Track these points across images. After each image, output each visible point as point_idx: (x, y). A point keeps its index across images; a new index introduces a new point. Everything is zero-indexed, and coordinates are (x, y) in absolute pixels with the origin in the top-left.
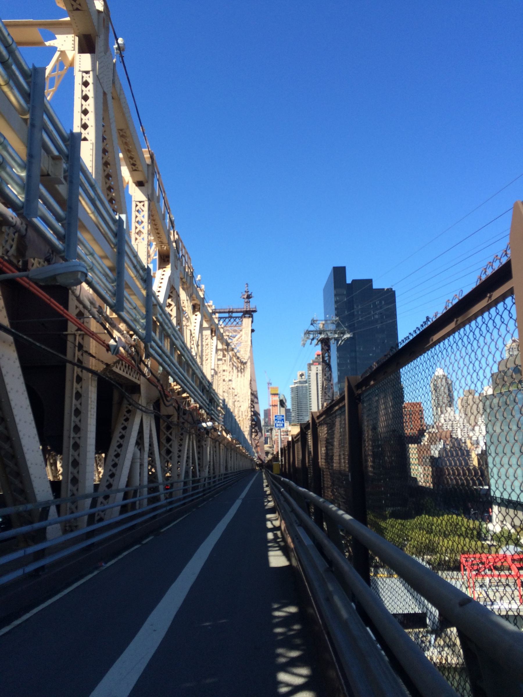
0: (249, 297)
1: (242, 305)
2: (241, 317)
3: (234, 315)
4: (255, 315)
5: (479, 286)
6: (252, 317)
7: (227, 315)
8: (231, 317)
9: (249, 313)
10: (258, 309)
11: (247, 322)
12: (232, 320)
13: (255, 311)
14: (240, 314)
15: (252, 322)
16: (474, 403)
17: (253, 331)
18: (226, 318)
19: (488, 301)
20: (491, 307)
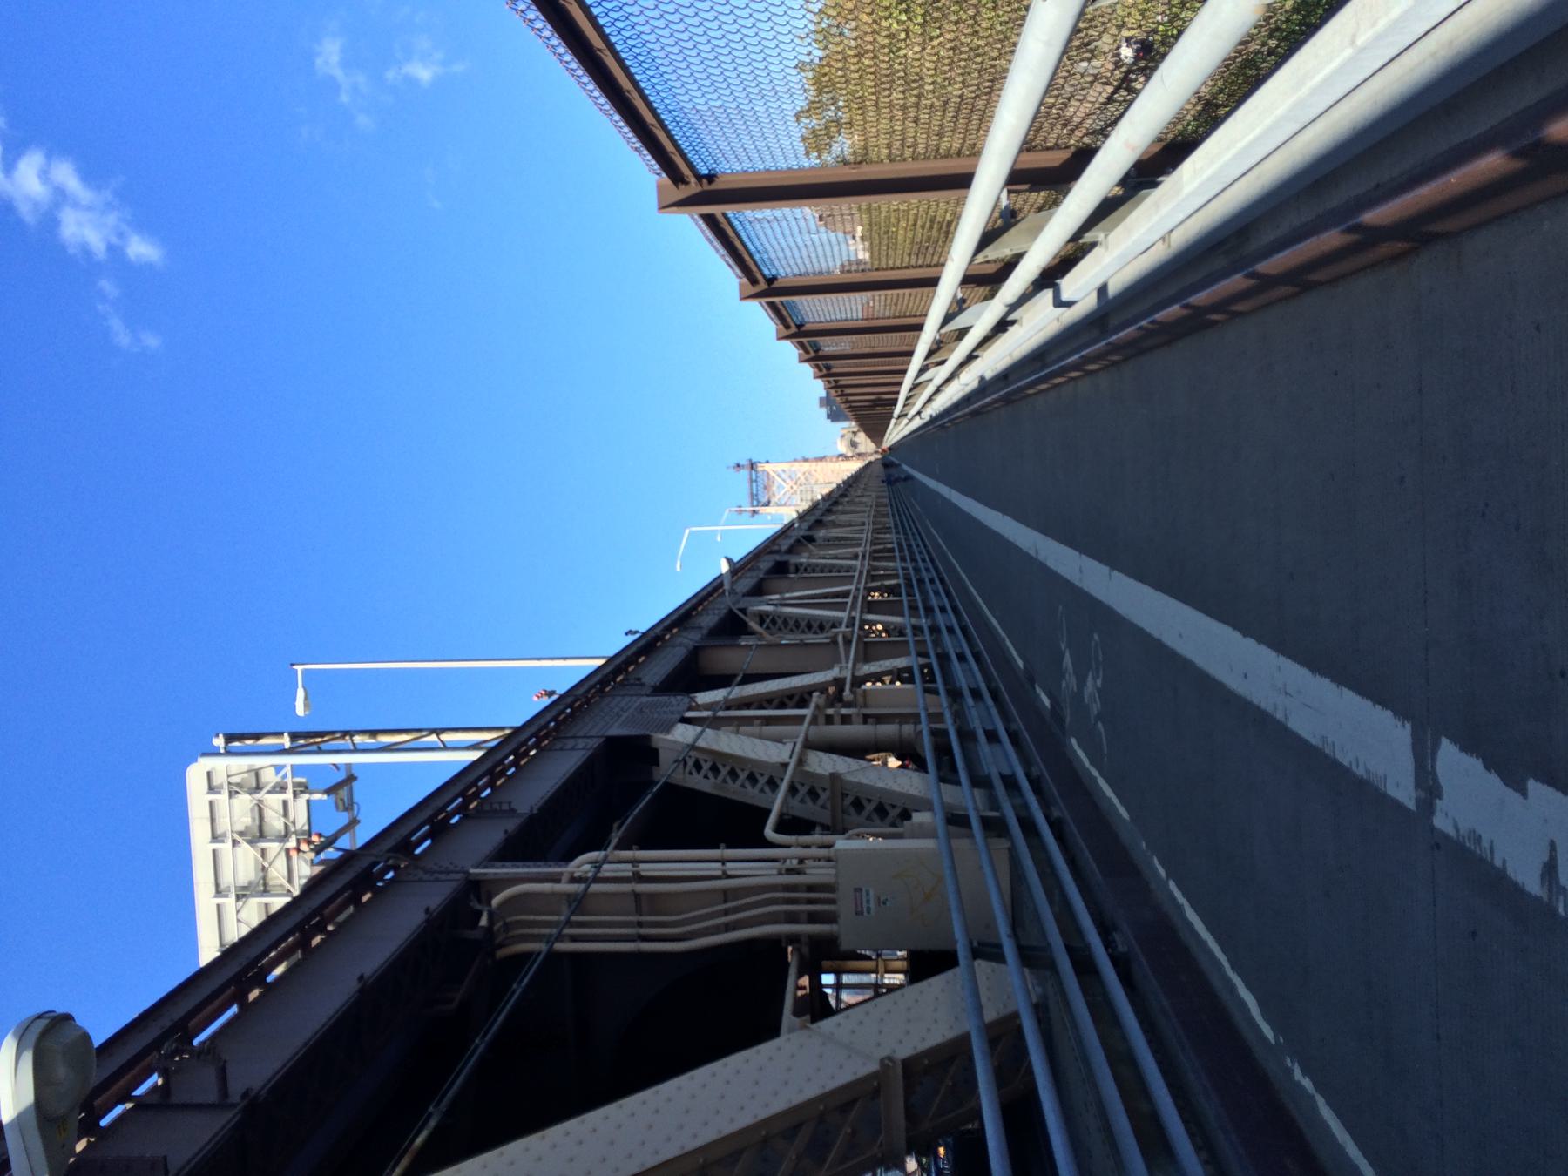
0: (738, 466)
1: (745, 473)
2: (756, 471)
3: (754, 477)
4: (754, 460)
5: (546, 18)
6: (755, 463)
7: (754, 485)
8: (756, 481)
9: (752, 466)
10: (749, 458)
11: (760, 468)
12: (758, 480)
13: (750, 460)
14: (753, 473)
15: (760, 463)
16: (765, 59)
17: (767, 462)
18: (757, 486)
19: (606, 55)
20: (615, 49)
